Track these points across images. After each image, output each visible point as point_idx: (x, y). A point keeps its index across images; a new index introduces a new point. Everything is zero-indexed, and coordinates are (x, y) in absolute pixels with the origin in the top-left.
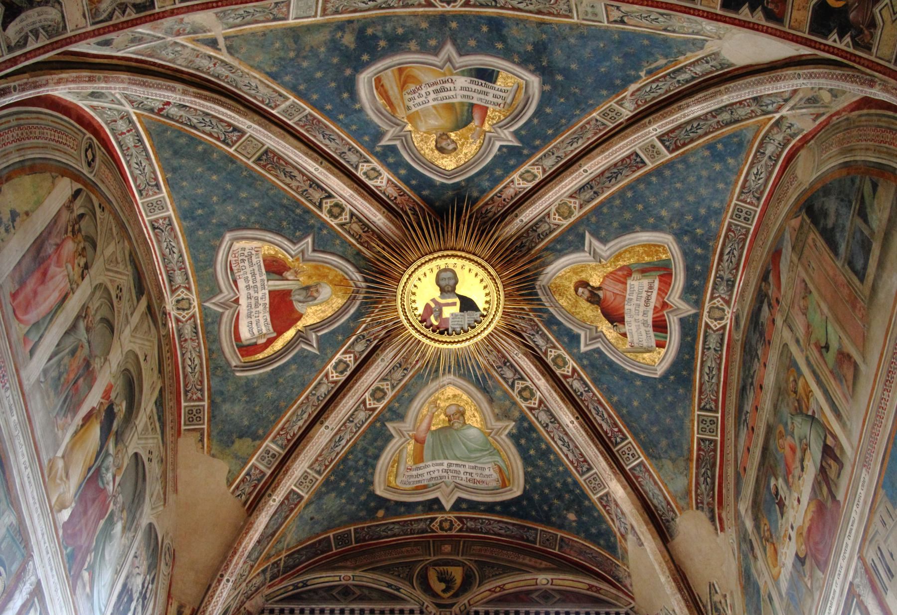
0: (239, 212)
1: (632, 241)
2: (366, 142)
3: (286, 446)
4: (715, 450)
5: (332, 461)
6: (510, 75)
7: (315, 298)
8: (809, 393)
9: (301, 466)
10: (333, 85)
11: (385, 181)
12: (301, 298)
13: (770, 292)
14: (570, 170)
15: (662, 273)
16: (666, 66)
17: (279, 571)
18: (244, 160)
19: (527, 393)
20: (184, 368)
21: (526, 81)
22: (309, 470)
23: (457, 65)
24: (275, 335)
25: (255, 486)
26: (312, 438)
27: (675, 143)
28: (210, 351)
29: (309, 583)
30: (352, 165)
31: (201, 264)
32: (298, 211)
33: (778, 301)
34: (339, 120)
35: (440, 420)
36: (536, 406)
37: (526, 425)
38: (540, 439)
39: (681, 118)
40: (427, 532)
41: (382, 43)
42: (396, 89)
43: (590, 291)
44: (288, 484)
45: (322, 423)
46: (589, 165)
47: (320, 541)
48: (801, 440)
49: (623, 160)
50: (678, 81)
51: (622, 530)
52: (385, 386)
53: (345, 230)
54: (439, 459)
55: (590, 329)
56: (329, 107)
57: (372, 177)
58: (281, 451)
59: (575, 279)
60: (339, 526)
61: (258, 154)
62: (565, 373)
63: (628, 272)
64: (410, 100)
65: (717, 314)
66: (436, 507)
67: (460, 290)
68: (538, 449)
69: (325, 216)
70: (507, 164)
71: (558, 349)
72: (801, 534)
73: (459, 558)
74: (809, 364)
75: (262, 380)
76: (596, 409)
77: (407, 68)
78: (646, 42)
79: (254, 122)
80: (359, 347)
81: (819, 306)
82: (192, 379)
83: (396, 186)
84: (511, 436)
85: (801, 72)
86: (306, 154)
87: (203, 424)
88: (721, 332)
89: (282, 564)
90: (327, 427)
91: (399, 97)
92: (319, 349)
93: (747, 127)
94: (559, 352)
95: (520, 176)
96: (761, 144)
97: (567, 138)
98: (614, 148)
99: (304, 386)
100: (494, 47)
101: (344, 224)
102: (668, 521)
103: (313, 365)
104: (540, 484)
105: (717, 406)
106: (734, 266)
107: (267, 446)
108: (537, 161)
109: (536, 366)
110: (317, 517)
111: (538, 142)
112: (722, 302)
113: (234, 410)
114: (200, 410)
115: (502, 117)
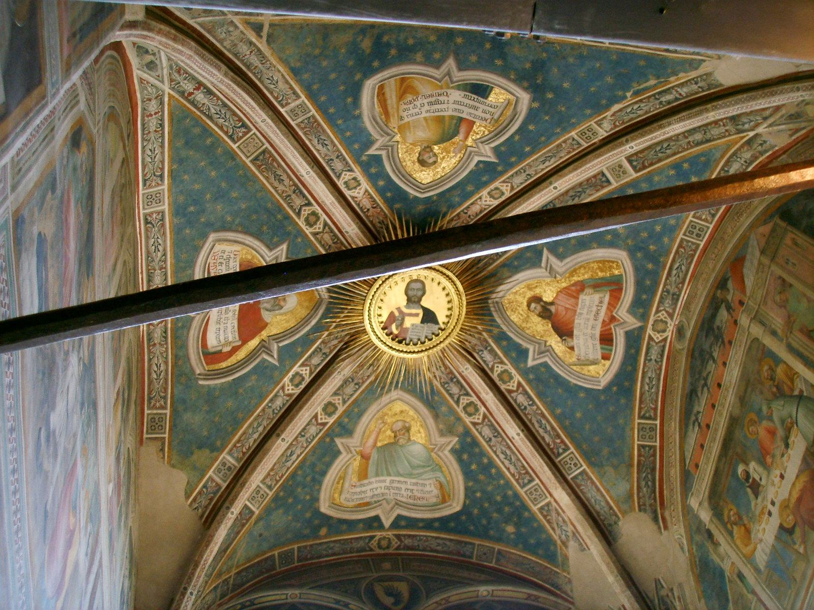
0: (227, 213)
1: (588, 257)
3: (241, 459)
4: (654, 455)
5: (283, 476)
6: (503, 91)
7: (282, 307)
8: (792, 375)
9: (256, 479)
10: (342, 88)
11: (362, 192)
12: (268, 306)
13: (729, 298)
14: (539, 187)
15: (613, 288)
16: (654, 87)
17: (228, 589)
18: (244, 158)
19: (471, 409)
20: (150, 374)
21: (517, 97)
22: (261, 485)
23: (455, 79)
24: (240, 343)
25: (211, 499)
26: (269, 450)
27: (643, 163)
28: (176, 357)
29: (256, 602)
30: (335, 173)
31: (182, 265)
32: (279, 216)
33: (741, 303)
34: (337, 125)
35: (386, 437)
36: (480, 421)
37: (469, 440)
38: (482, 454)
39: (660, 135)
40: (366, 551)
41: (393, 52)
42: (394, 100)
43: (542, 306)
44: (243, 499)
45: (279, 435)
46: (560, 181)
47: (266, 559)
48: (783, 421)
49: (588, 180)
50: (661, 103)
51: (563, 537)
52: (337, 400)
53: (317, 239)
55: (539, 344)
56: (332, 110)
57: (351, 187)
58: (236, 464)
59: (529, 294)
60: (284, 544)
61: (255, 154)
62: (510, 388)
63: (581, 287)
64: (404, 110)
65: (661, 326)
66: (375, 524)
67: (425, 302)
68: (479, 464)
69: (301, 223)
71: (505, 364)
72: (787, 507)
73: (401, 574)
74: (791, 349)
75: (222, 388)
76: (539, 422)
78: (642, 63)
79: (269, 116)
80: (315, 361)
81: (805, 295)
82: (156, 386)
83: (372, 197)
84: (453, 451)
85: (800, 85)
86: (302, 156)
87: (165, 433)
88: (662, 344)
89: (232, 579)
90: (283, 440)
92: (280, 359)
93: (716, 147)
94: (505, 367)
95: (489, 193)
96: (728, 161)
97: (541, 156)
98: (588, 166)
99: (262, 398)
101: (317, 233)
102: (610, 525)
103: (271, 377)
104: (480, 498)
105: (656, 414)
106: (681, 280)
107: (224, 458)
108: (508, 178)
109: (484, 381)
110: (266, 534)
111: (513, 159)
112: (666, 315)
113: (194, 419)
114: (162, 418)
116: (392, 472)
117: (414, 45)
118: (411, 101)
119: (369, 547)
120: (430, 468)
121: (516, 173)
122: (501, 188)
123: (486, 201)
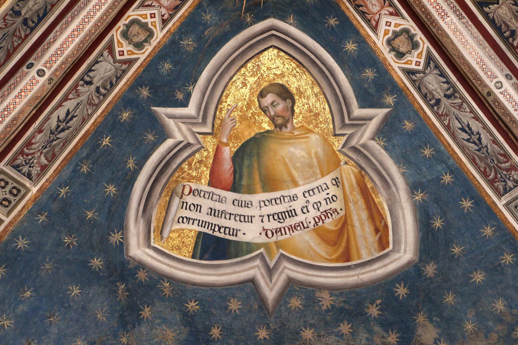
2: (409, 119)
6: (174, 254)
10: (457, 250)
11: (382, 27)
21: (149, 246)
23: (258, 262)
30: (437, 66)
34: (452, 172)
41: (374, 311)
46: (36, 88)
56: (467, 204)
64: (333, 199)
70: (175, 63)
77: (337, 260)
83: (363, 14)
91: (351, 205)
97: (78, 130)
100: (201, 303)
108: (124, 72)
111: (126, 115)
115: (185, 166)
117: (338, 321)
118: (326, 216)
121: (113, 86)
122: (131, 48)
123: (153, 16)
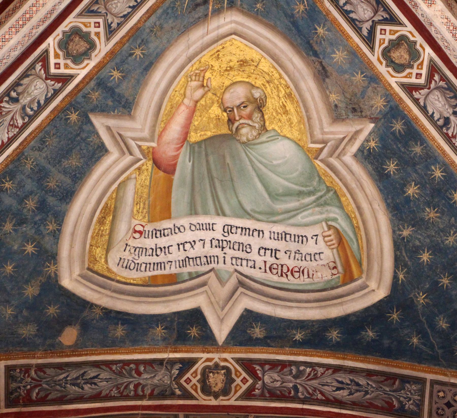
36: (422, 81)
37: (398, 126)
40: (172, 395)
54: (206, 213)
66: (194, 332)
104: (431, 266)
116: (227, 211)
119: (181, 387)
120: (313, 198)
